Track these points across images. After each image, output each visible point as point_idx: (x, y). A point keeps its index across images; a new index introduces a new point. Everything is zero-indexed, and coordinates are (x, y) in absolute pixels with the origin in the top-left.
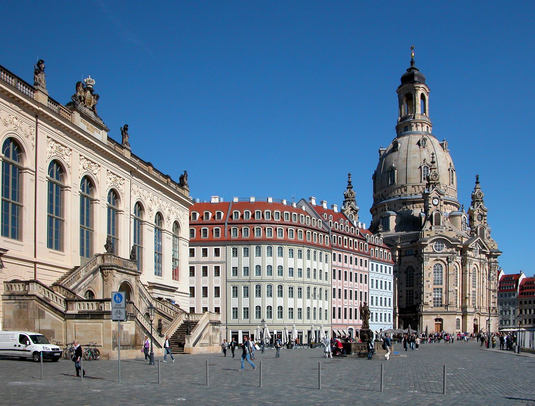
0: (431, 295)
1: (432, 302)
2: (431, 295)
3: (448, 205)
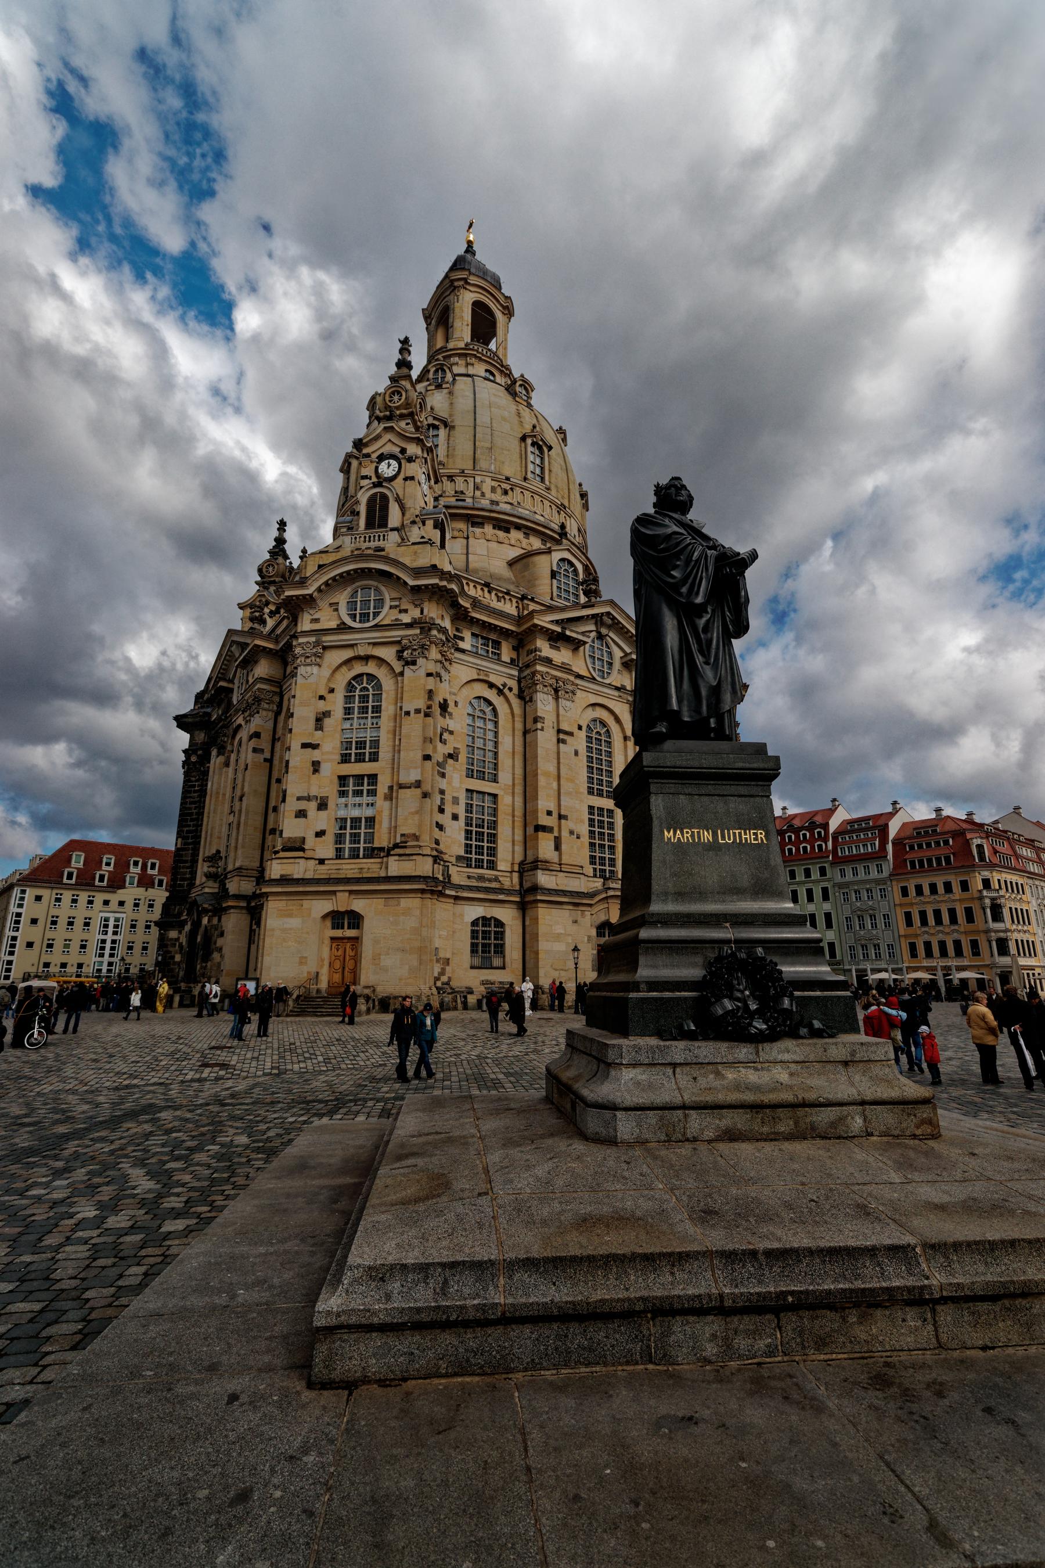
0: (323, 805)
1: (329, 838)
2: (323, 805)
3: (515, 535)
